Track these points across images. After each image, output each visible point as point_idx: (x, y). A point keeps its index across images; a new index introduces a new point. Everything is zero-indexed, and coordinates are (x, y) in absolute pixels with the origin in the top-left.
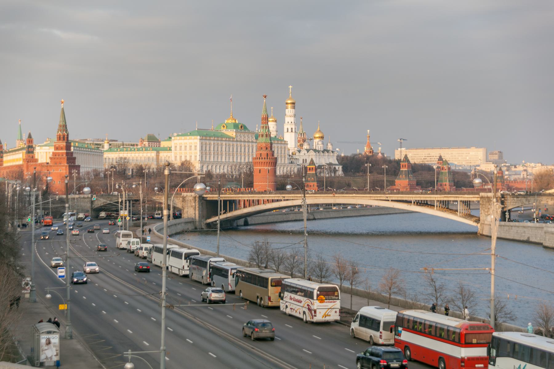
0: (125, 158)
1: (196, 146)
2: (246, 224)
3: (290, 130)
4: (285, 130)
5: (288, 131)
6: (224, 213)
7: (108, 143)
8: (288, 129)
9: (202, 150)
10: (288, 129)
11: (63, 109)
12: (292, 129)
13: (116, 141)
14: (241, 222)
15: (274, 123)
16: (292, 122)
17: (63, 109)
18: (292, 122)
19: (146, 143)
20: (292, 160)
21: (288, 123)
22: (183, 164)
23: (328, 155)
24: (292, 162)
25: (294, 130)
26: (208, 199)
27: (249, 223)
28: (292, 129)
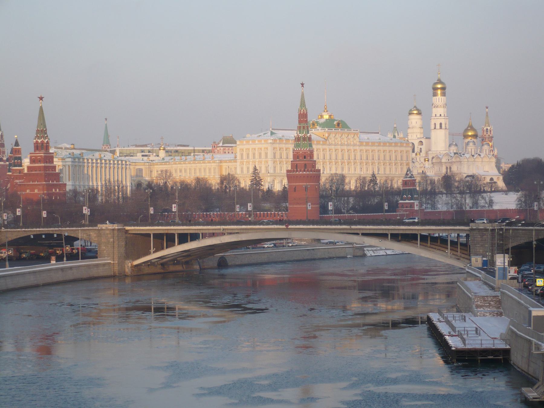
0: (166, 171)
1: (266, 154)
2: (222, 264)
3: (438, 126)
4: (432, 127)
5: (435, 128)
6: (154, 252)
7: (164, 149)
8: (435, 124)
9: (275, 157)
10: (435, 124)
11: (41, 108)
12: (441, 124)
13: (188, 146)
14: (212, 261)
15: (418, 117)
16: (440, 115)
17: (41, 108)
18: (440, 115)
19: (220, 149)
20: (422, 168)
21: (436, 116)
22: (223, 179)
23: (482, 161)
24: (423, 171)
25: (443, 126)
26: (130, 232)
27: (230, 264)
28: (441, 124)
